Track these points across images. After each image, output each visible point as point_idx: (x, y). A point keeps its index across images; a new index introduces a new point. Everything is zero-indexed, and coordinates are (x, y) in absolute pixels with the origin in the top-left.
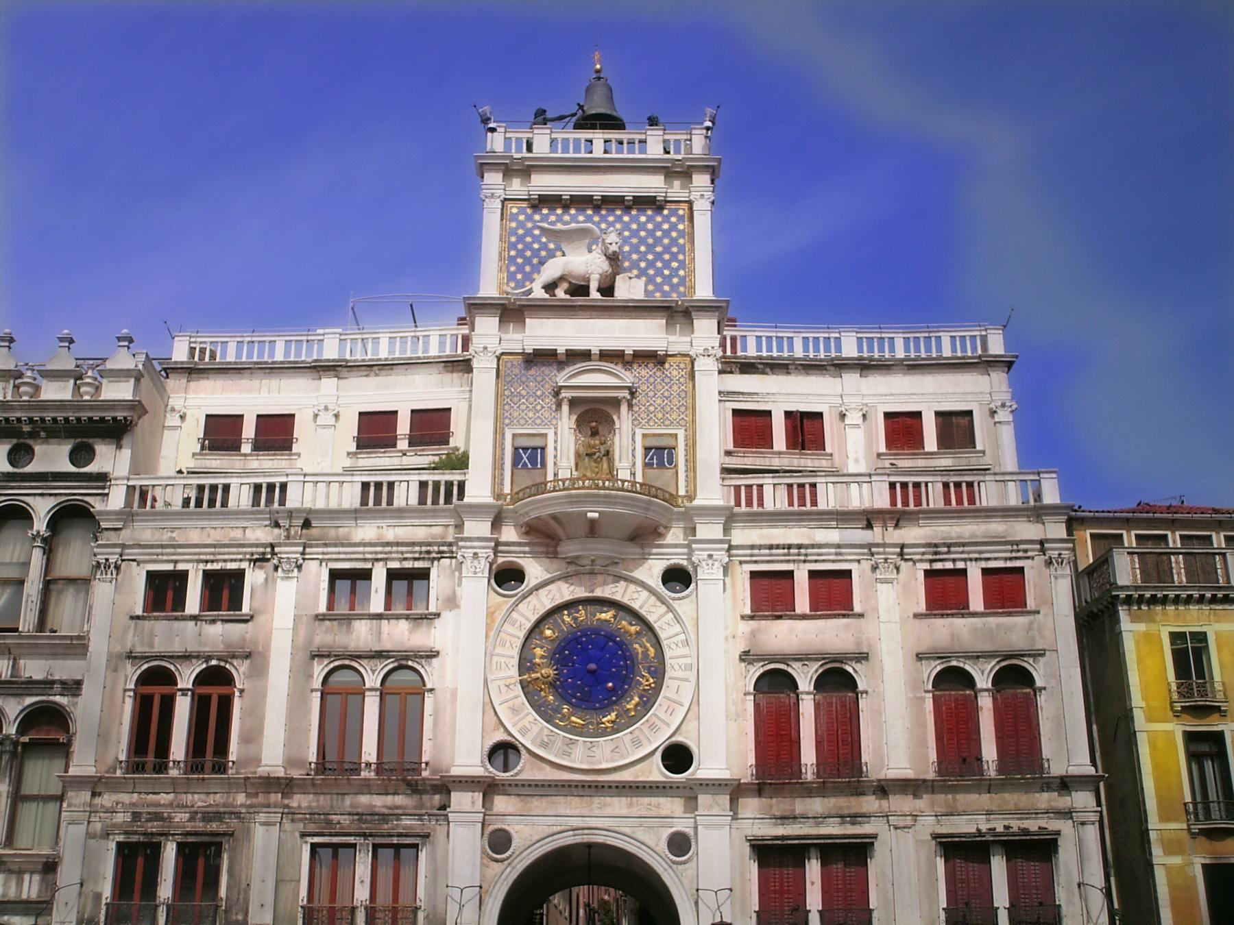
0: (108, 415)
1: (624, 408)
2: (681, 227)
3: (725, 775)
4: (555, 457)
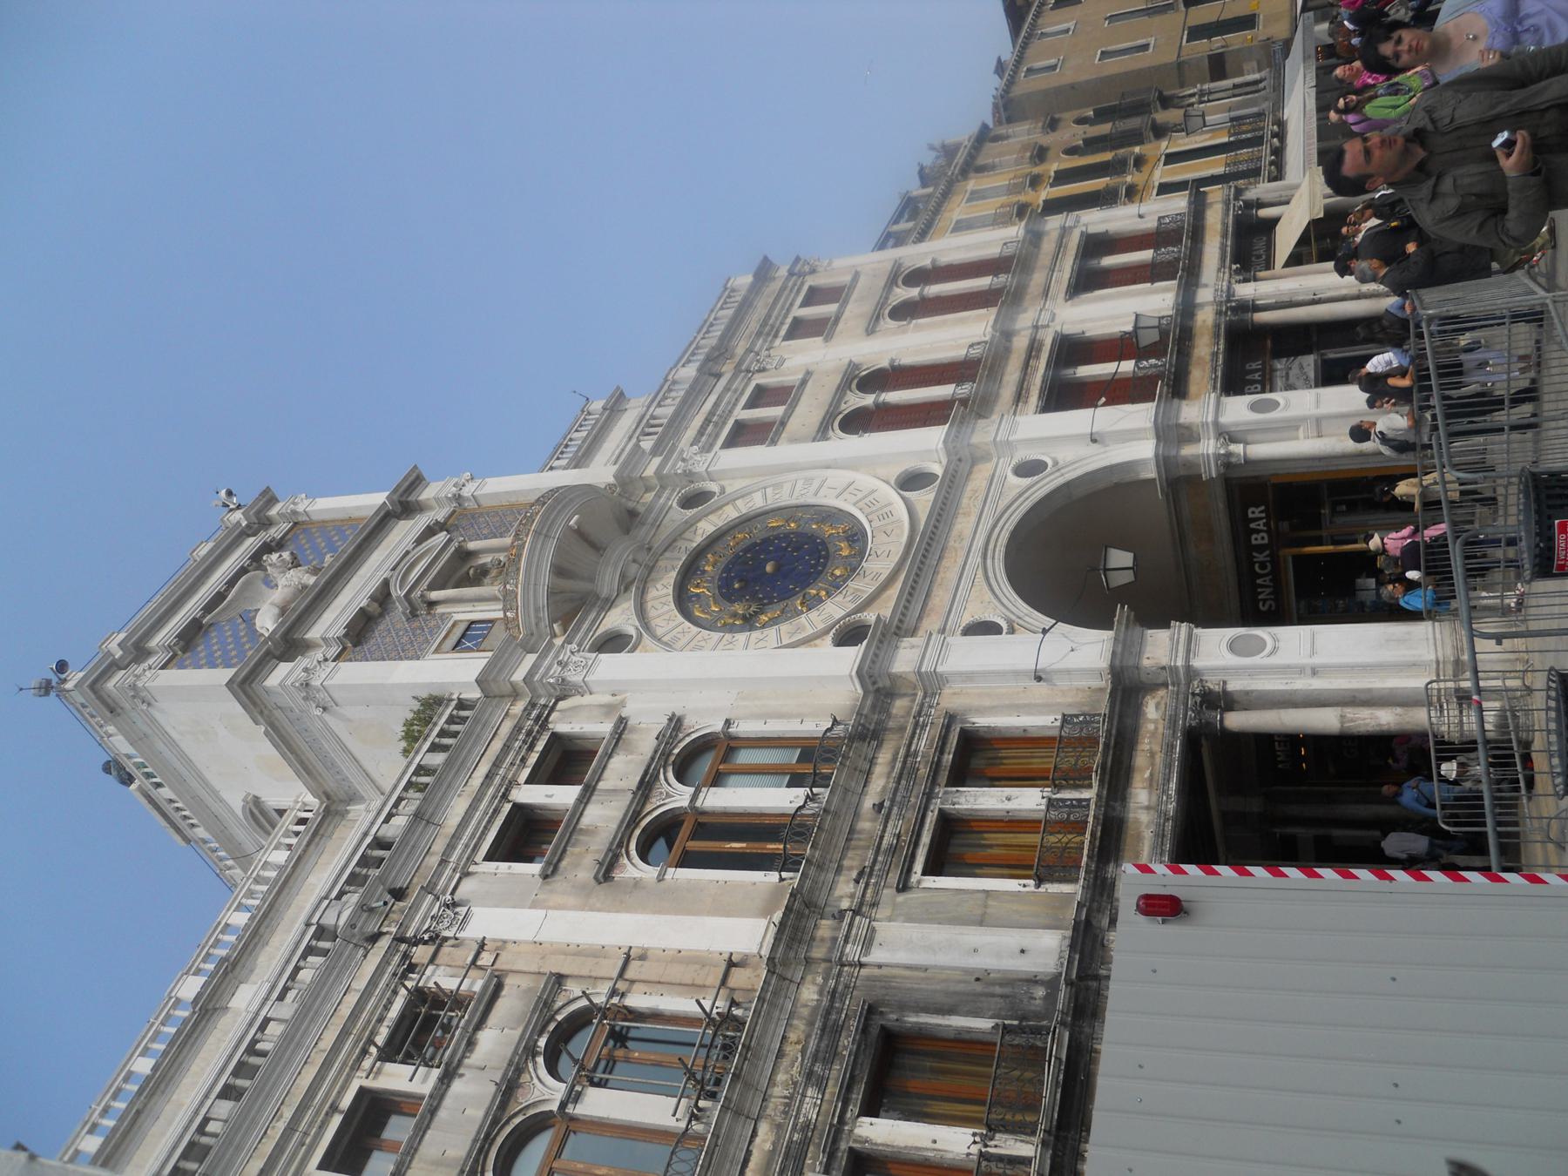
1: (472, 546)
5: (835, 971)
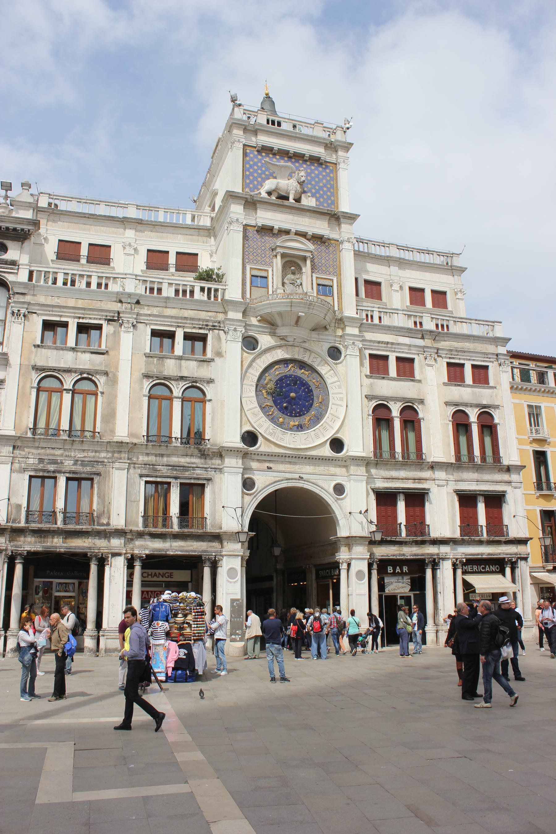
0: (19, 227)
1: (308, 262)
2: (332, 175)
3: (364, 455)
4: (273, 283)
5: (110, 461)
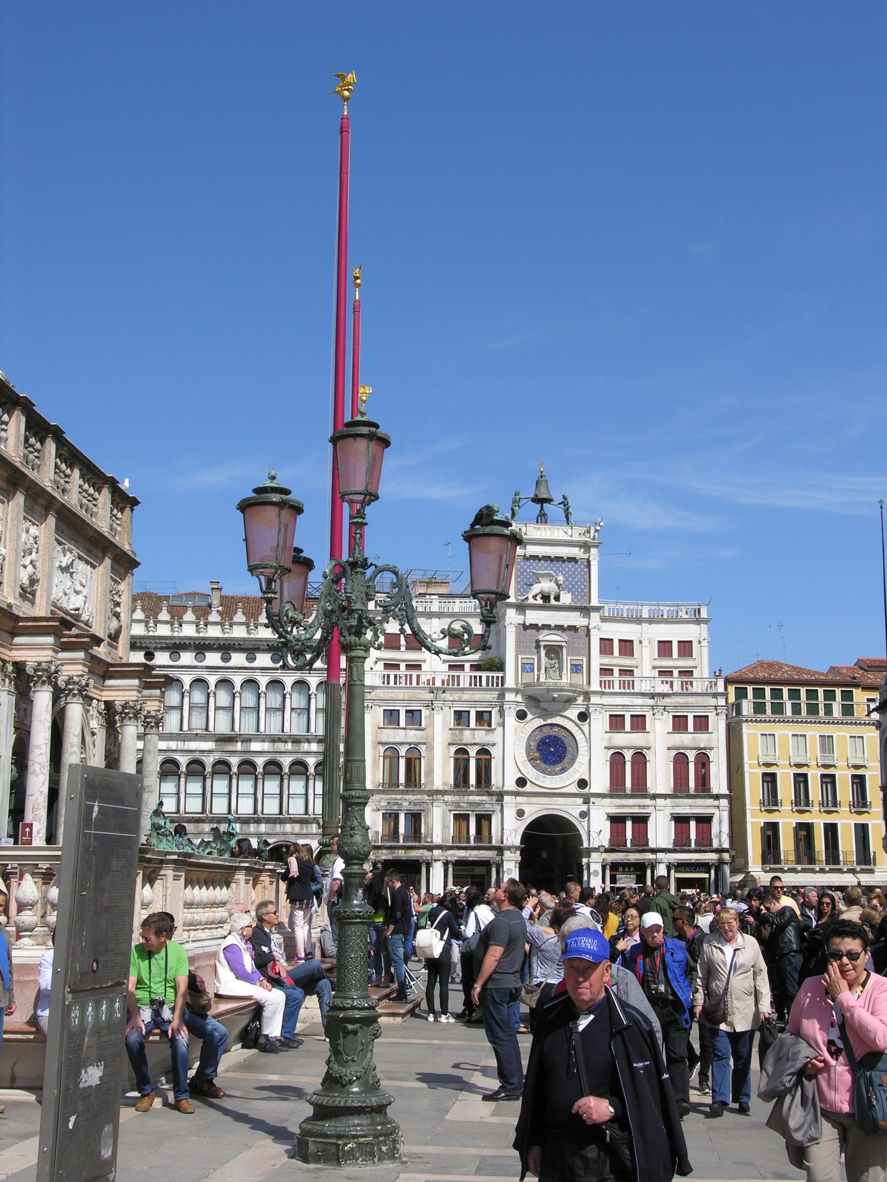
1: (565, 651)
